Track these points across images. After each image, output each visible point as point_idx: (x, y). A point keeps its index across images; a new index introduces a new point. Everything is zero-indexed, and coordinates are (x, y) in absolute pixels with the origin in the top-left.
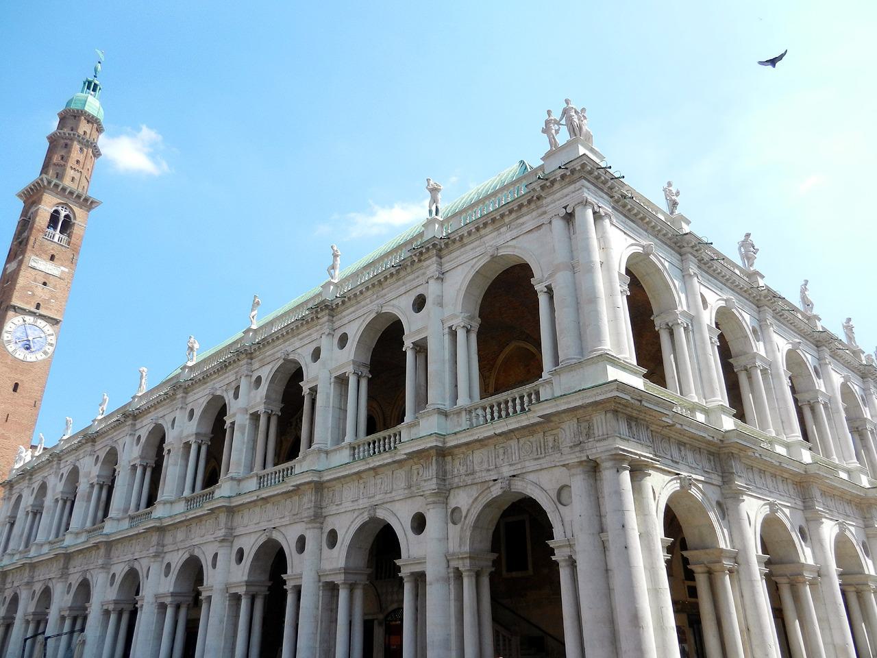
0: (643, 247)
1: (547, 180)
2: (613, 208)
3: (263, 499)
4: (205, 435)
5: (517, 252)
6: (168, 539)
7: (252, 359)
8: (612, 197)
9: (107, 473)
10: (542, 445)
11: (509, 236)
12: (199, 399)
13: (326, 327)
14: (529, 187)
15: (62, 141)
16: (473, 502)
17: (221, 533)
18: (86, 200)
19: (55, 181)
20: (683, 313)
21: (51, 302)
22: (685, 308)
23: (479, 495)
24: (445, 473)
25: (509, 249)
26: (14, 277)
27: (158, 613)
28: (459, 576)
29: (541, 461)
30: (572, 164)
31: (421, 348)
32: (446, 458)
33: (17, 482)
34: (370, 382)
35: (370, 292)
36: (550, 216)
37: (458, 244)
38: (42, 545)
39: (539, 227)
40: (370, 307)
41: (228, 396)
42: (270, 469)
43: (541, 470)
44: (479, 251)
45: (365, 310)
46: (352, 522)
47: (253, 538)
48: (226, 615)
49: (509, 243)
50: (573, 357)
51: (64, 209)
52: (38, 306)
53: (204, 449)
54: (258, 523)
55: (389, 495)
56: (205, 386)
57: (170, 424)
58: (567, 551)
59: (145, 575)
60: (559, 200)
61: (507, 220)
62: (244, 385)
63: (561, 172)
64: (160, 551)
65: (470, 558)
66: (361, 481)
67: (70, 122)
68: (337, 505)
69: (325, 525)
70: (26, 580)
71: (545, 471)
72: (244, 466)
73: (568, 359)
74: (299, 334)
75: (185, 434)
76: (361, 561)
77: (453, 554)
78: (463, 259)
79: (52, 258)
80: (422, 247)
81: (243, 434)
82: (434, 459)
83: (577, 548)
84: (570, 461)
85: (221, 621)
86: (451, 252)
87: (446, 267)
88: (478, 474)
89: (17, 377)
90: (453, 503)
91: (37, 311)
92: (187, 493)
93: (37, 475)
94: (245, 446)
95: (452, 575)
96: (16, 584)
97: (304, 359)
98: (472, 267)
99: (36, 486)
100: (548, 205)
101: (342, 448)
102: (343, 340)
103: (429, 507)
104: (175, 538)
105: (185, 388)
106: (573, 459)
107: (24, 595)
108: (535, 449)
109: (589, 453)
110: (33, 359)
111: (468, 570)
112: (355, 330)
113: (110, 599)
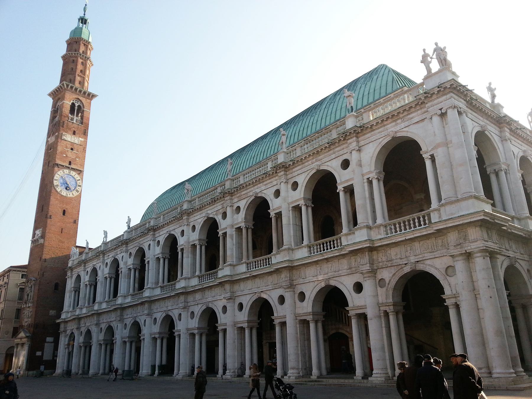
0: (481, 127)
1: (429, 93)
2: (467, 107)
3: (253, 276)
4: (204, 240)
5: (409, 135)
6: (190, 298)
7: (232, 196)
8: (465, 100)
9: (138, 262)
10: (435, 245)
11: (403, 125)
12: (199, 219)
13: (283, 178)
14: (417, 97)
15: (71, 59)
16: (393, 276)
17: (228, 295)
18: (89, 94)
19: (71, 85)
20: (504, 163)
21: (76, 160)
22: (504, 161)
23: (397, 272)
24: (373, 260)
25: (404, 133)
26: (55, 146)
27: (189, 338)
28: (386, 314)
29: (435, 253)
30: (445, 84)
31: (350, 191)
32: (372, 253)
33: (75, 268)
34: (313, 209)
35: (311, 158)
36: (431, 114)
37: (369, 130)
38: (101, 303)
39: (423, 120)
40: (312, 166)
41: (219, 218)
42: (251, 259)
43: (434, 258)
44: (383, 134)
45: (308, 168)
46: (314, 288)
47: (248, 297)
48: (236, 338)
49: (404, 129)
50: (452, 196)
51: (77, 102)
52: (70, 163)
53: (203, 248)
54: (251, 289)
55: (337, 273)
56: (201, 212)
57: (179, 234)
58: (453, 301)
59: (177, 318)
60: (436, 105)
61: (401, 116)
62: (229, 211)
63: (439, 89)
64: (186, 305)
65: (393, 305)
66: (317, 266)
67: (75, 46)
68: (303, 279)
69: (296, 290)
70: (95, 322)
71: (437, 259)
72: (236, 258)
73: (449, 198)
74: (263, 182)
75: (191, 239)
76: (319, 309)
77: (383, 303)
78: (372, 139)
79: (74, 133)
80: (347, 132)
81: (232, 239)
82: (367, 253)
83: (461, 298)
84: (455, 254)
85: (234, 342)
86: (364, 135)
87: (362, 143)
88: (394, 261)
89: (65, 207)
90: (379, 277)
91: (69, 166)
92: (197, 273)
93: (89, 263)
94: (235, 246)
95: (383, 314)
96: (87, 324)
97: (269, 195)
98: (380, 143)
99: (89, 269)
100: (429, 108)
101: (303, 247)
102: (295, 186)
103: (365, 279)
104: (195, 298)
105: (188, 213)
106: (456, 252)
107: (94, 330)
108: (430, 247)
109: (466, 249)
110: (71, 196)
111: (392, 312)
112: (303, 180)
113: (156, 331)
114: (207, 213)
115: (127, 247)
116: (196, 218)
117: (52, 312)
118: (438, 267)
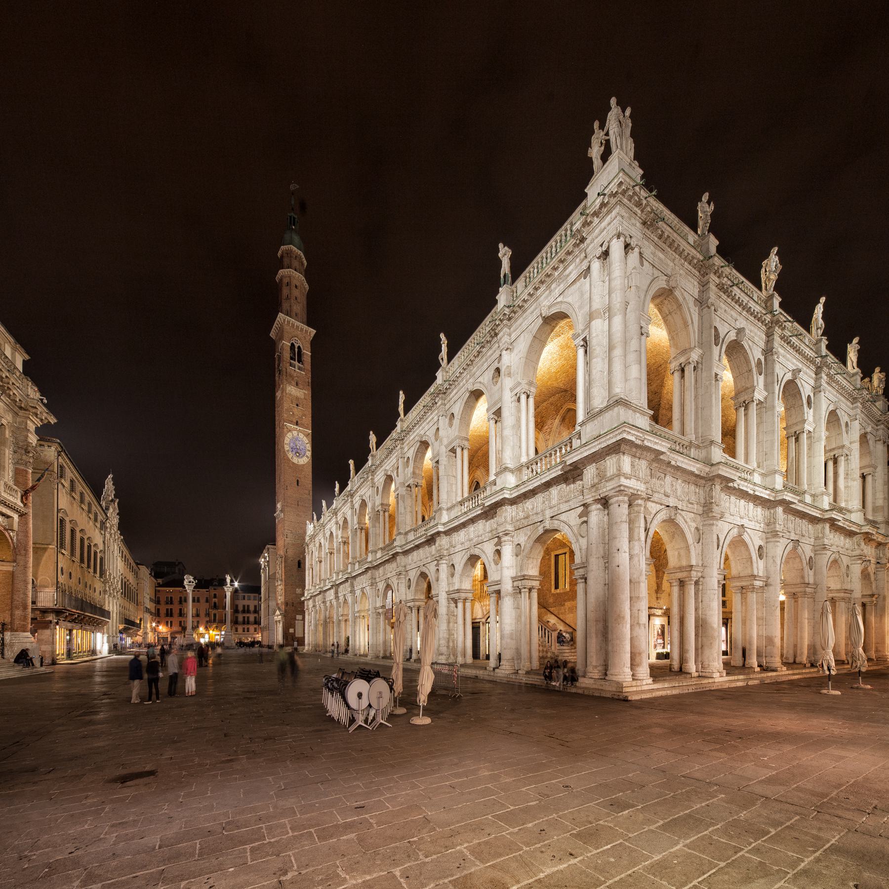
57: (368, 499)
114: (385, 470)
115: (336, 518)
116: (379, 477)
117: (298, 591)
118: (572, 524)
